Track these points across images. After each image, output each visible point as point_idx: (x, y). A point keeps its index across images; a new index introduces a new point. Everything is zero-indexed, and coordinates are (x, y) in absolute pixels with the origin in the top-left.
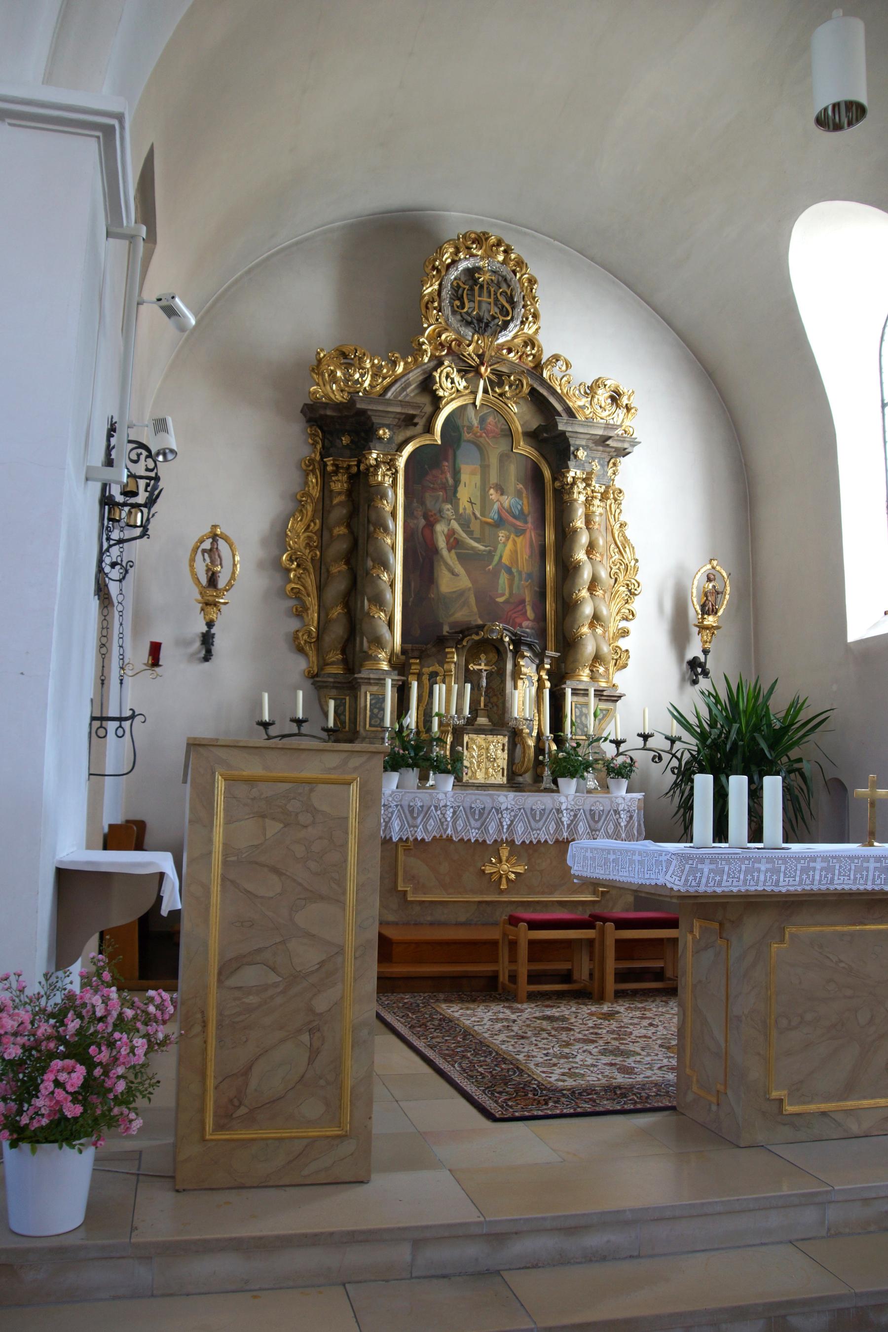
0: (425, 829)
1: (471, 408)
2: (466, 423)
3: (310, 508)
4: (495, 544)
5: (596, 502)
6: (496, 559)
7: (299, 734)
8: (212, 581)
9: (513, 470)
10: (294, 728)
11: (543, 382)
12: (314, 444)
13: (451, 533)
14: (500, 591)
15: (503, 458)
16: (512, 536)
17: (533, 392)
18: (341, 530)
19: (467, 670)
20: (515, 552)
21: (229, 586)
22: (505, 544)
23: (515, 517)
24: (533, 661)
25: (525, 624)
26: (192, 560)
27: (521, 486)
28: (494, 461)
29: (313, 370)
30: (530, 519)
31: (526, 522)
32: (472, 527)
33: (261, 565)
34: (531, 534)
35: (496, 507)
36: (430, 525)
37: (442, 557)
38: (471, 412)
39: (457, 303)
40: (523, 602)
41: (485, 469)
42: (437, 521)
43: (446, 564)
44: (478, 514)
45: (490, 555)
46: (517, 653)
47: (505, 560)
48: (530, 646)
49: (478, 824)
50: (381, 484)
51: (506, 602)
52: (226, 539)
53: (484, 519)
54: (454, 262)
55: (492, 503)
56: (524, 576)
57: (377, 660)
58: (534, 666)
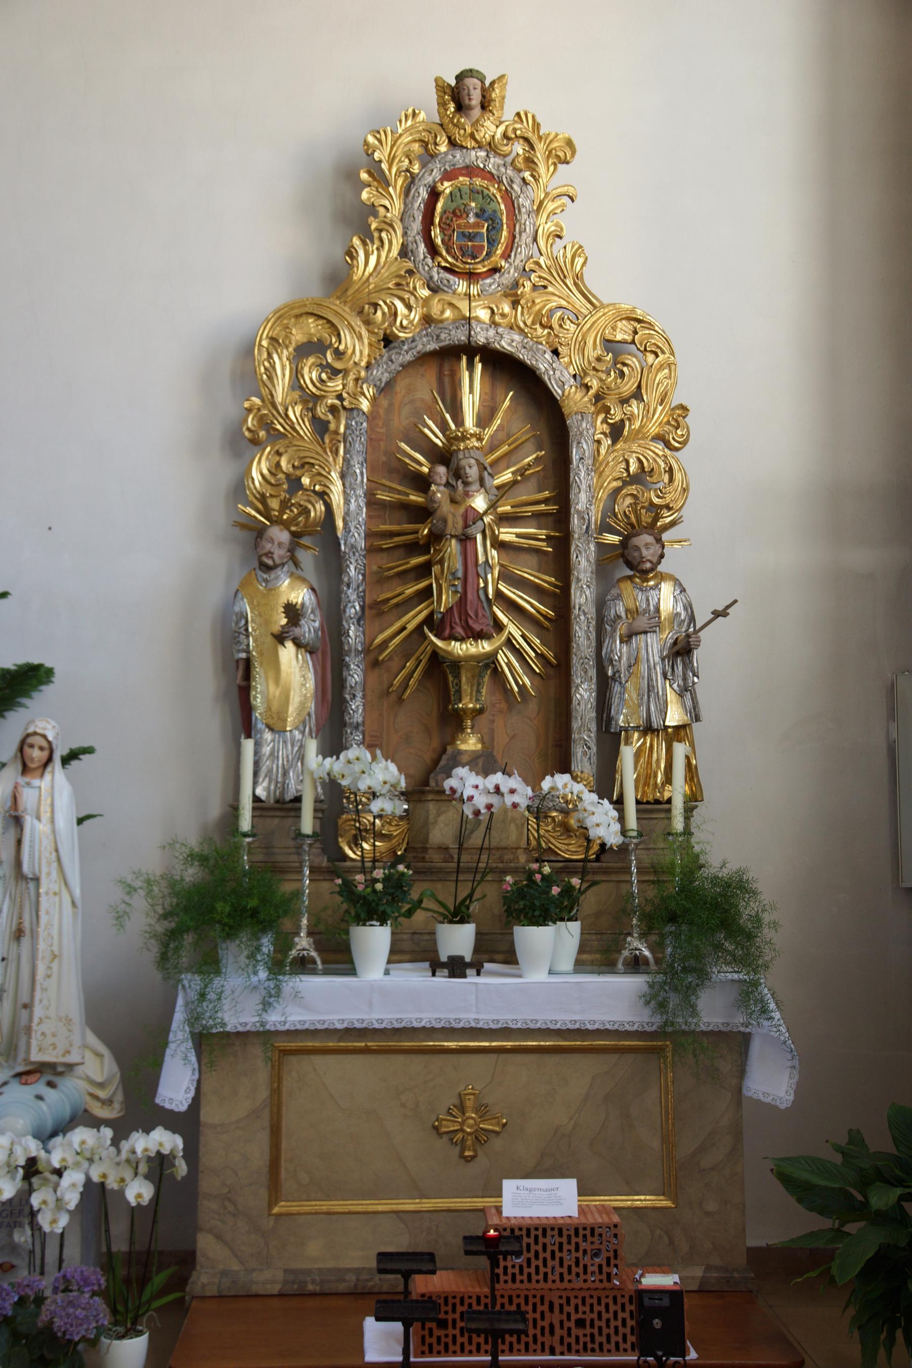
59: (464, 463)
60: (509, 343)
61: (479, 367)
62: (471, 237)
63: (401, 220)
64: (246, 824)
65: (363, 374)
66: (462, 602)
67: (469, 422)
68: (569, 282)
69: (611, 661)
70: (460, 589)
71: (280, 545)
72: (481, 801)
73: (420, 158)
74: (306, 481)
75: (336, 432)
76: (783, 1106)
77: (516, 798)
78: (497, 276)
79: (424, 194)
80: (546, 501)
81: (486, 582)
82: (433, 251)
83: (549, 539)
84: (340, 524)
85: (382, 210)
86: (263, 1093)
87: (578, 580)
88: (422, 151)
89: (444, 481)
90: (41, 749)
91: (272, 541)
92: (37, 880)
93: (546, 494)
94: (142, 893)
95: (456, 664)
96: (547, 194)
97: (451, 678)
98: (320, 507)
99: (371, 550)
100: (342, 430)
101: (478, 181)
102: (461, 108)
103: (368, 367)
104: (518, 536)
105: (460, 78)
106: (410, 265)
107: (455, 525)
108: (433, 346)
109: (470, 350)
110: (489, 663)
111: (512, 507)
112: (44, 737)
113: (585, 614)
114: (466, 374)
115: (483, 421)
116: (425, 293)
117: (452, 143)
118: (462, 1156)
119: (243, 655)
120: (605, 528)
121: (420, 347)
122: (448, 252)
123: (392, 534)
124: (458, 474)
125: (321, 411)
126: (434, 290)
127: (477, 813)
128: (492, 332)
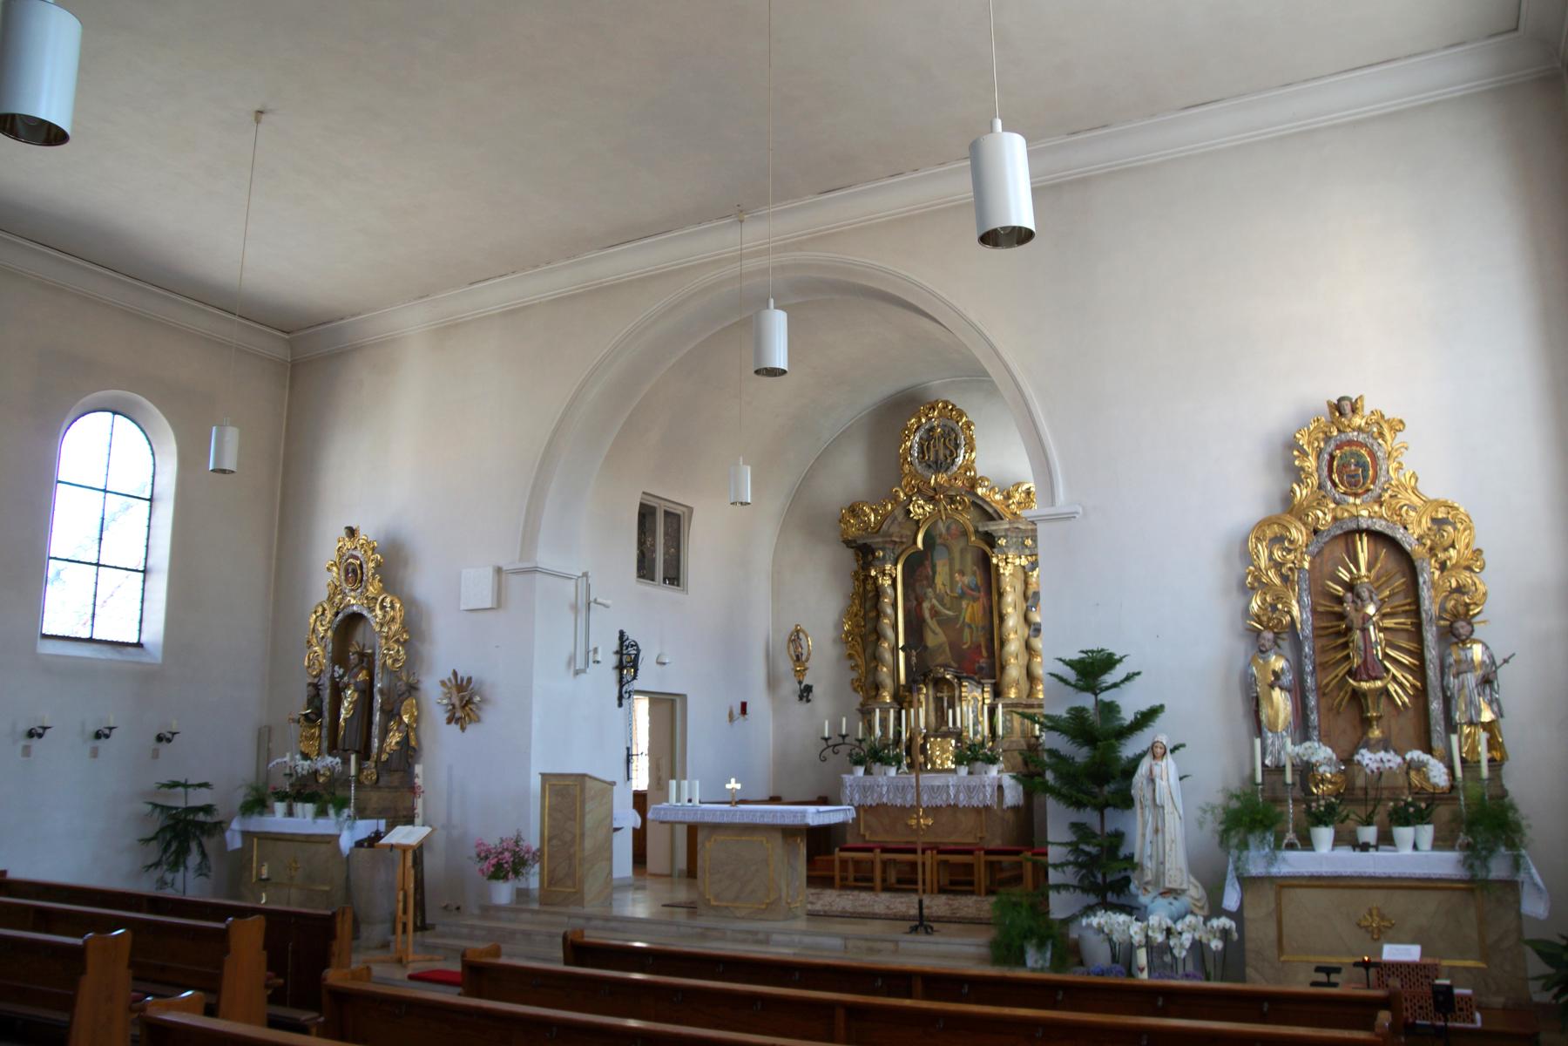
0: (872, 798)
1: (940, 521)
2: (938, 533)
3: (857, 601)
4: (960, 610)
6: (961, 619)
7: (844, 743)
8: (798, 658)
9: (969, 558)
10: (840, 740)
12: (857, 561)
13: (933, 607)
14: (965, 641)
15: (962, 551)
16: (971, 603)
20: (973, 613)
21: (807, 660)
22: (966, 609)
23: (972, 590)
24: (977, 687)
25: (982, 661)
26: (789, 648)
27: (975, 568)
28: (957, 555)
29: (840, 522)
30: (982, 589)
31: (979, 592)
32: (945, 601)
33: (835, 641)
34: (983, 599)
36: (920, 604)
37: (928, 624)
38: (941, 525)
40: (980, 646)
42: (923, 601)
43: (931, 629)
44: (948, 592)
45: (957, 617)
46: (961, 685)
47: (967, 620)
49: (901, 796)
50: (883, 585)
51: (969, 648)
52: (804, 632)
53: (952, 595)
55: (957, 582)
56: (980, 629)
58: (980, 690)
59: (1360, 590)
60: (1379, 526)
61: (1365, 539)
62: (1353, 477)
63: (1317, 471)
64: (1259, 779)
65: (1304, 550)
66: (1365, 661)
67: (1363, 571)
68: (1410, 491)
69: (1449, 688)
70: (1363, 655)
71: (1268, 640)
72: (1374, 766)
73: (1323, 439)
74: (1280, 606)
75: (1293, 581)
76: (1542, 918)
77: (1391, 764)
78: (1370, 493)
79: (1326, 456)
80: (1409, 604)
81: (1377, 651)
82: (1334, 485)
83: (1412, 623)
84: (1299, 626)
85: (1306, 468)
86: (1273, 905)
87: (1428, 646)
88: (1324, 436)
89: (1351, 600)
90: (1161, 748)
91: (1264, 638)
92: (1163, 807)
93: (1409, 601)
94: (1210, 813)
96: (1392, 449)
97: (1363, 700)
98: (1288, 618)
99: (1316, 636)
100: (1296, 579)
101: (1354, 448)
102: (1341, 414)
103: (1307, 546)
104: (1396, 623)
105: (1339, 400)
106: (1323, 493)
107: (1357, 622)
108: (1339, 532)
109: (1360, 531)
111: (1391, 608)
112: (1162, 743)
113: (1433, 664)
114: (1359, 543)
115: (1369, 568)
116: (1332, 505)
117: (1339, 430)
118: (1373, 938)
119: (1255, 695)
120: (1441, 618)
121: (1332, 534)
122: (1342, 485)
123: (1327, 628)
124: (1358, 596)
126: (1337, 503)
127: (1372, 772)
128: (1370, 522)
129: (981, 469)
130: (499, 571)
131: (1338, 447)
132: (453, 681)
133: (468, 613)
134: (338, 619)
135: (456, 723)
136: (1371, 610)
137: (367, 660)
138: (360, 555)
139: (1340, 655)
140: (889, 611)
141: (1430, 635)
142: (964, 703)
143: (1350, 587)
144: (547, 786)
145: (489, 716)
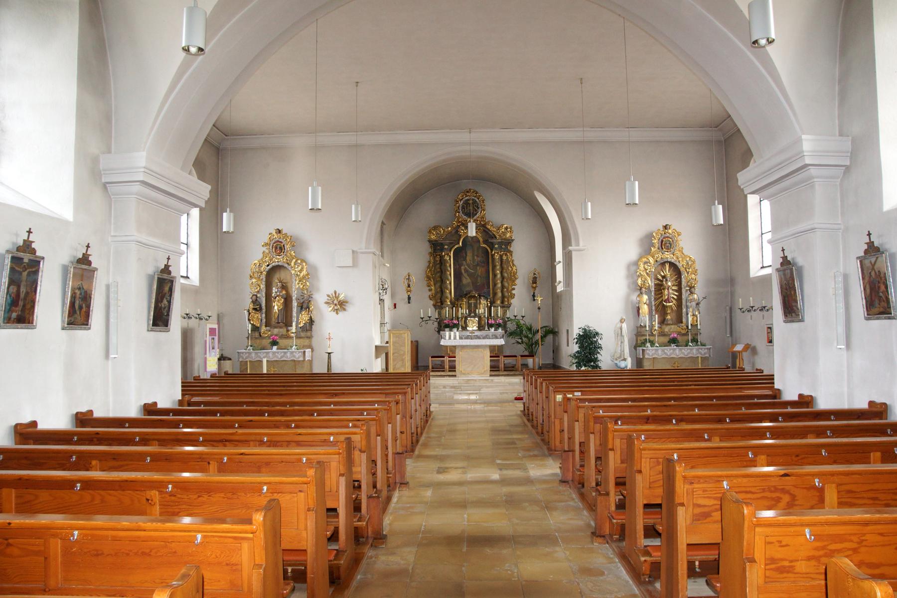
5: (504, 256)
8: (409, 286)
10: (428, 319)
11: (487, 228)
17: (484, 231)
18: (439, 270)
19: (468, 303)
20: (481, 271)
35: (476, 261)
36: (460, 266)
39: (463, 210)
41: (473, 251)
42: (462, 266)
46: (480, 298)
47: (479, 274)
48: (484, 296)
54: (462, 199)
57: (446, 302)
60: (673, 261)
66: (668, 298)
82: (662, 249)
95: (667, 307)
102: (666, 229)
109: (667, 262)
110: (671, 306)
117: (665, 233)
124: (666, 280)
125: (648, 271)
126: (663, 254)
129: (488, 219)
130: (353, 252)
131: (664, 238)
132: (334, 295)
133: (339, 269)
134: (269, 267)
135: (334, 311)
136: (669, 284)
137: (284, 287)
138: (283, 241)
139: (660, 296)
140: (449, 269)
141: (684, 291)
142: (481, 305)
143: (664, 277)
144: (392, 335)
145: (350, 309)
